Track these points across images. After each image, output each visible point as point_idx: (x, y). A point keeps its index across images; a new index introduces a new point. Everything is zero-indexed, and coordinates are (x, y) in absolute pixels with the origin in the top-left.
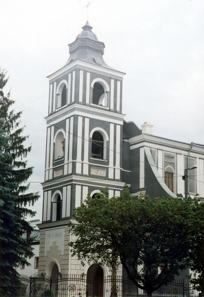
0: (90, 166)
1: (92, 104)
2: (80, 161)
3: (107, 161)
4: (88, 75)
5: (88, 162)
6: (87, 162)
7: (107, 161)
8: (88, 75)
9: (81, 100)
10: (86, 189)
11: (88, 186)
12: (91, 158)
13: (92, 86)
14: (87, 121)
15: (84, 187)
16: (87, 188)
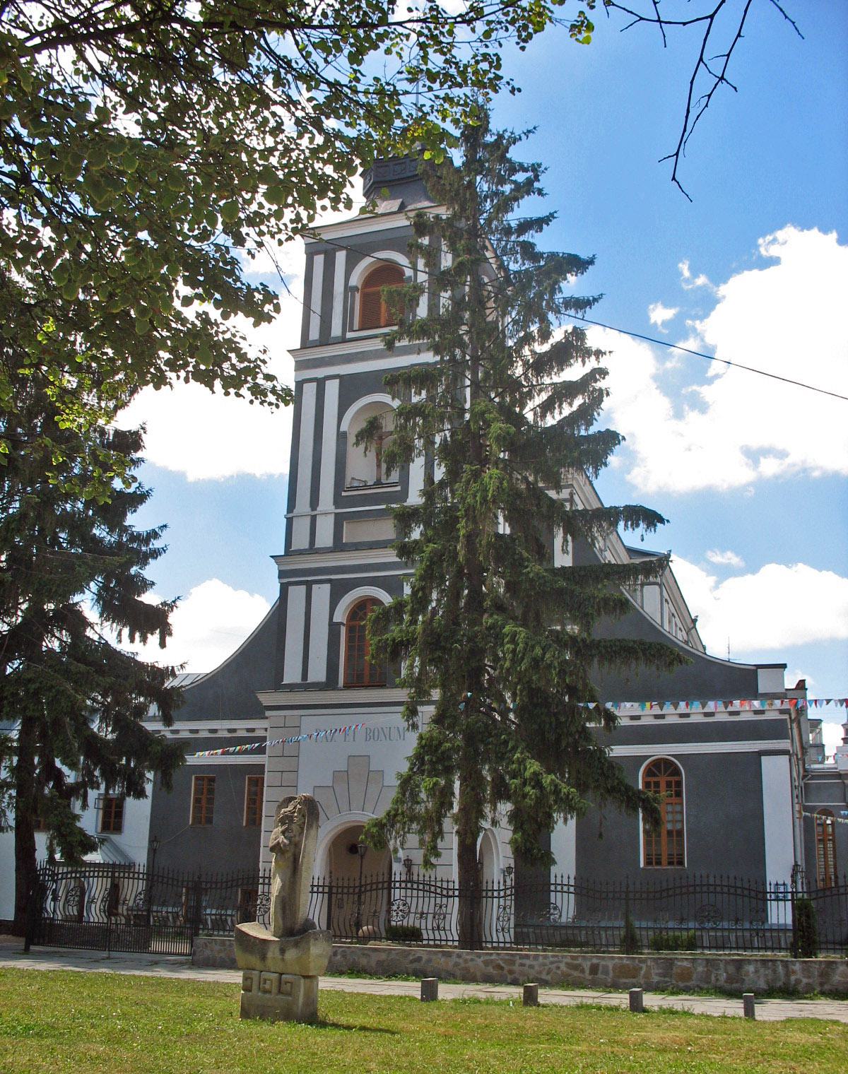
0: (339, 520)
1: (349, 335)
2: (307, 509)
3: (398, 488)
4: (341, 257)
5: (333, 507)
6: (332, 508)
7: (398, 488)
8: (341, 257)
9: (314, 335)
10: (322, 593)
11: (329, 581)
12: (344, 494)
13: (355, 280)
14: (332, 388)
15: (315, 587)
16: (327, 587)
